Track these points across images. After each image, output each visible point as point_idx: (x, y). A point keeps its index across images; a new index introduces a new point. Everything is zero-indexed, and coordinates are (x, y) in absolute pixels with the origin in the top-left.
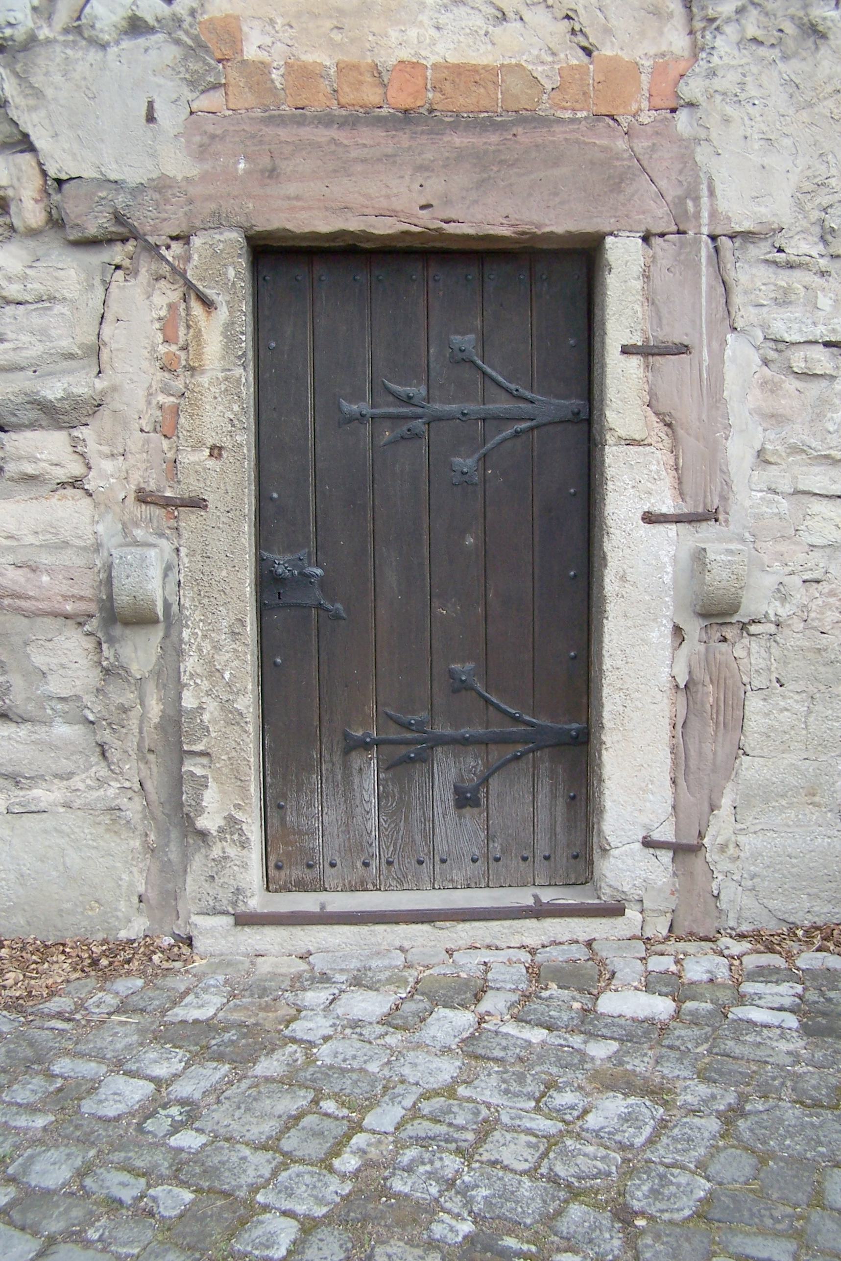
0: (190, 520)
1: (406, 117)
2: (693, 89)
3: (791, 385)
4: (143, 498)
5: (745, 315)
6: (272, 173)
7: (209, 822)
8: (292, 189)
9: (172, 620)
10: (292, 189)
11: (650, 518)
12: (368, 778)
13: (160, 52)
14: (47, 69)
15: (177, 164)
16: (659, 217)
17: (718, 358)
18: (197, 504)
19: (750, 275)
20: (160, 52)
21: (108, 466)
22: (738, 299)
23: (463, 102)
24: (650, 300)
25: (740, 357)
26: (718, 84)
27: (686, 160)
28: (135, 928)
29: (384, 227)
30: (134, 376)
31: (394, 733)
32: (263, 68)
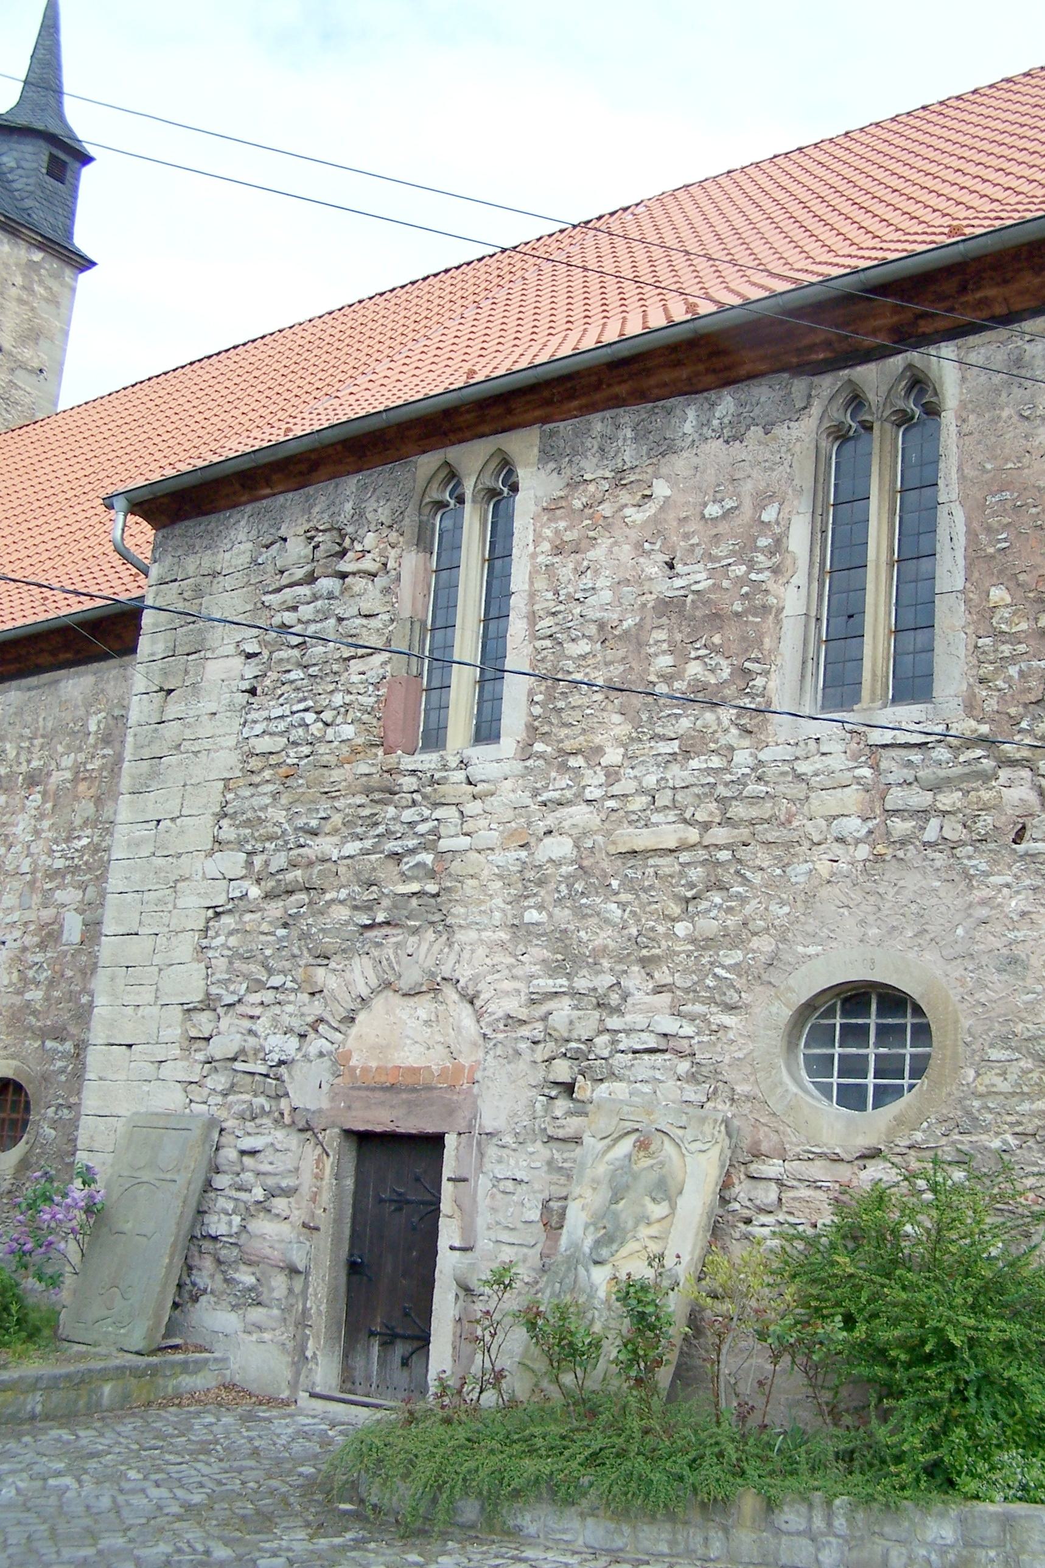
0: (315, 1234)
1: (392, 1088)
2: (478, 1076)
3: (499, 1196)
4: (304, 1225)
5: (488, 1167)
6: (349, 1108)
7: (309, 1354)
8: (354, 1114)
9: (307, 1273)
10: (354, 1114)
11: (452, 1248)
12: (376, 1349)
13: (326, 1062)
14: (296, 1069)
15: (325, 1104)
16: (462, 1126)
17: (476, 1182)
18: (317, 1229)
19: (492, 1151)
20: (326, 1062)
21: (297, 1212)
22: (485, 1160)
23: (410, 1080)
24: (457, 1158)
25: (484, 1183)
26: (486, 1073)
27: (475, 1103)
28: (285, 1395)
29: (379, 1129)
30: (306, 1181)
31: (384, 1330)
32: (354, 1069)
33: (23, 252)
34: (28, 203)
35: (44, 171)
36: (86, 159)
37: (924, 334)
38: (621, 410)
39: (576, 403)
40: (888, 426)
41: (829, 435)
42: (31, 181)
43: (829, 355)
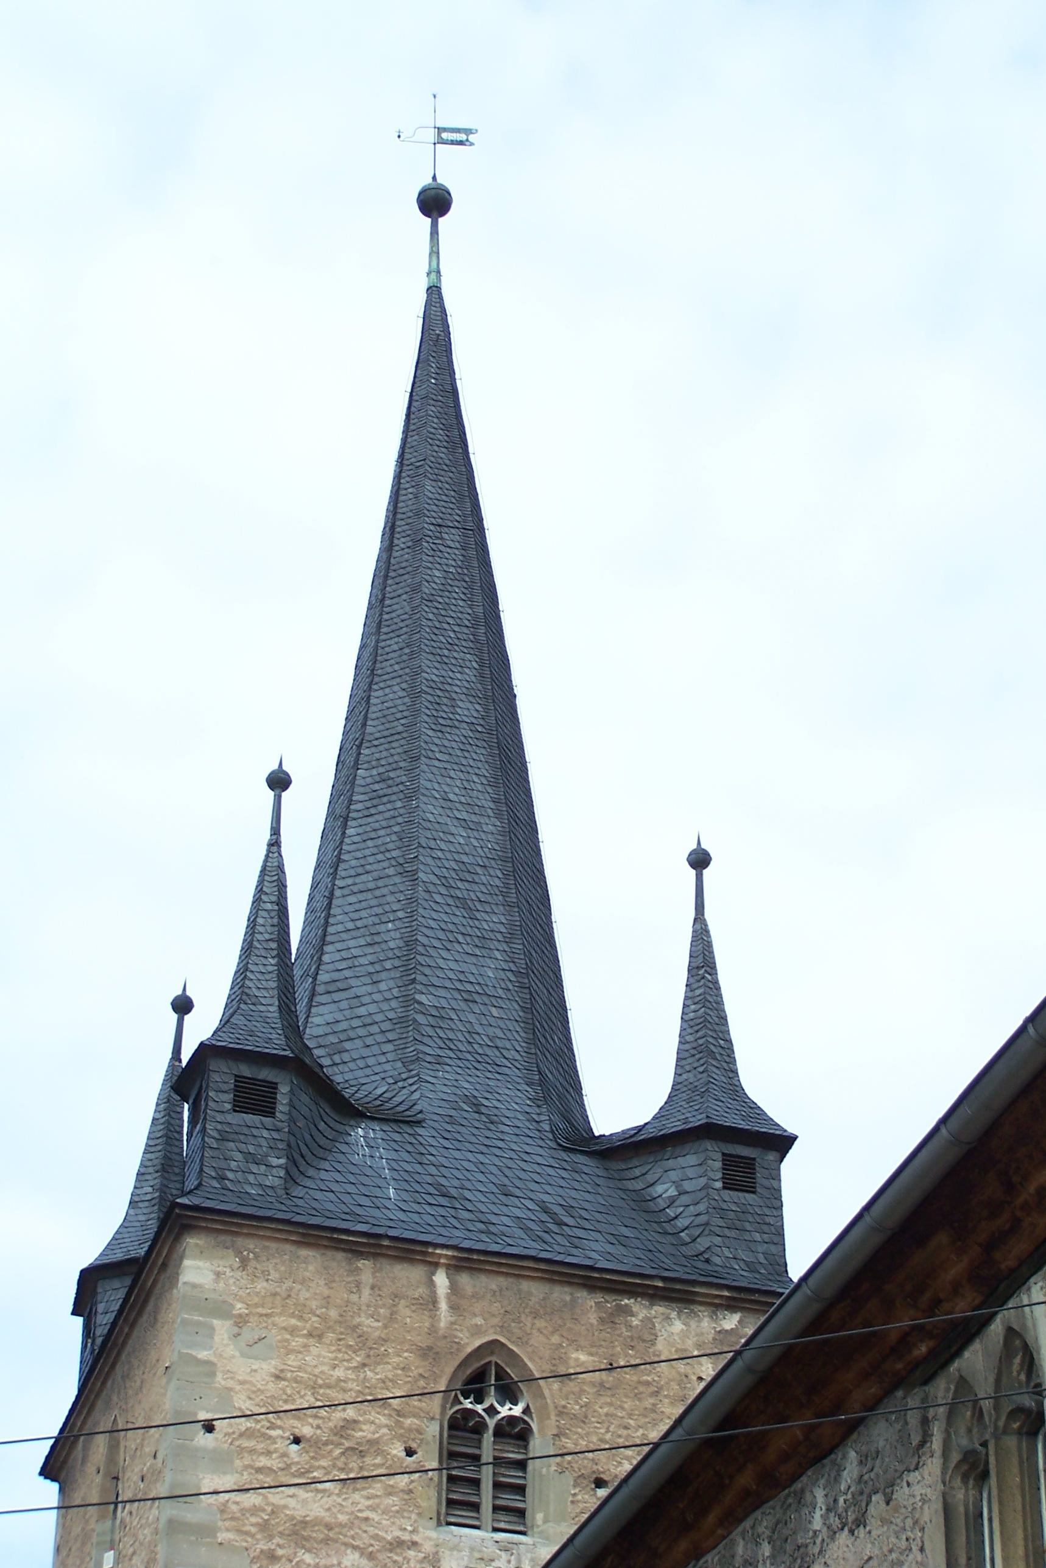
33: (706, 1323)
34: (703, 1243)
35: (719, 1185)
36: (783, 1143)
37: (1012, 1271)
38: (758, 1514)
39: (711, 1518)
40: (1011, 1442)
41: (965, 1478)
42: (702, 1207)
43: (932, 1343)
